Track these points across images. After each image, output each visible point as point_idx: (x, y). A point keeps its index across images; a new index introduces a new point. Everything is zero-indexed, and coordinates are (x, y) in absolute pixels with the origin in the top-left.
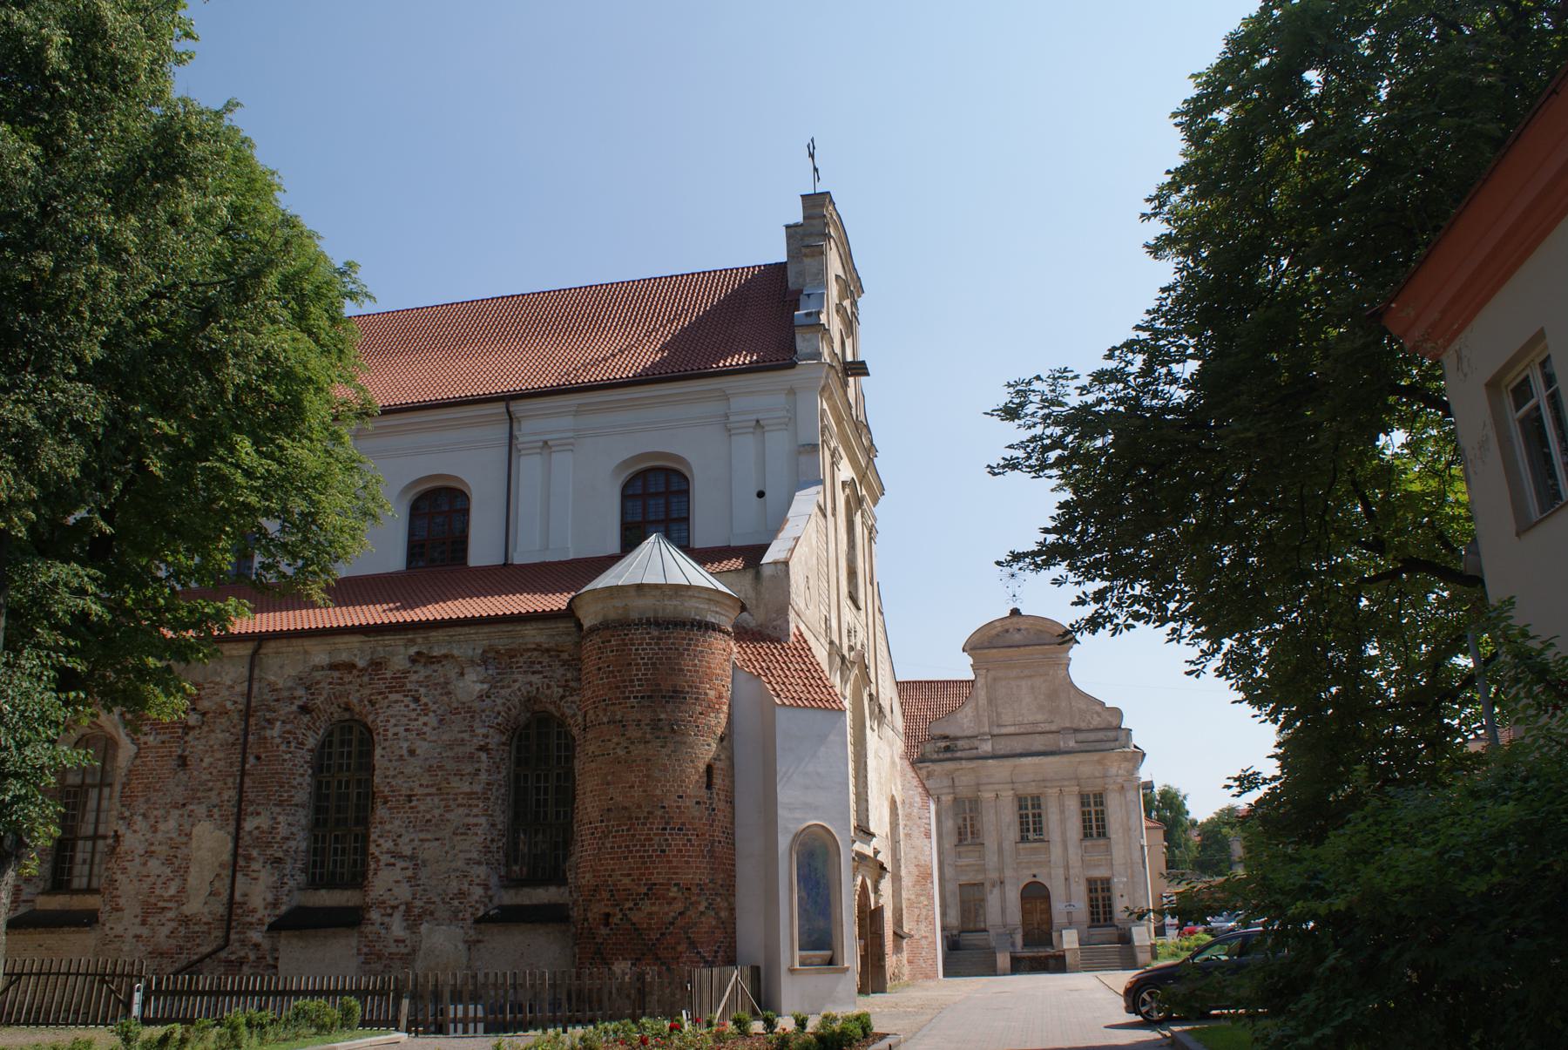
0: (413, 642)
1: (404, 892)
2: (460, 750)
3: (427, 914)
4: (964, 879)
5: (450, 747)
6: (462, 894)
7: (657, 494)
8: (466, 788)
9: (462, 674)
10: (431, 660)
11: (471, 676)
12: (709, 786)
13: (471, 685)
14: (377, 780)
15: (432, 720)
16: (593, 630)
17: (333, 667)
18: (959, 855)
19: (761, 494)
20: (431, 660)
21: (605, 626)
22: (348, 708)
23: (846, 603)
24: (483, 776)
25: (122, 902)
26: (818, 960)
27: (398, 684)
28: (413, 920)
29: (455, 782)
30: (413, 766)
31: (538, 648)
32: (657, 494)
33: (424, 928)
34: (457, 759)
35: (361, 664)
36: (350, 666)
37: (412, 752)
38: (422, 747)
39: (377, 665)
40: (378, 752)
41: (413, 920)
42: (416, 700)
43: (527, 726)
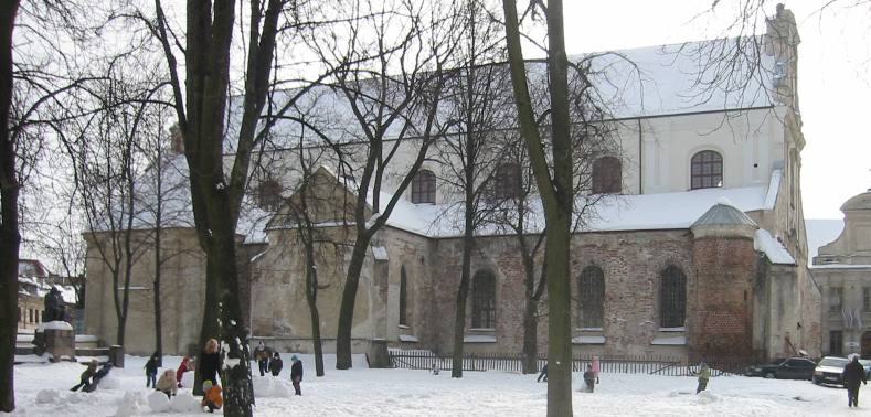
0: (620, 237)
1: (620, 333)
2: (641, 280)
3: (631, 341)
4: (834, 328)
5: (638, 278)
6: (644, 335)
7: (707, 163)
8: (644, 294)
9: (641, 251)
10: (628, 244)
11: (645, 251)
12: (745, 299)
13: (646, 255)
14: (607, 290)
15: (630, 269)
16: (700, 239)
17: (587, 246)
18: (831, 316)
19: (756, 166)
20: (628, 244)
21: (707, 238)
22: (592, 262)
23: (790, 209)
24: (651, 290)
25: (506, 334)
26: (840, 363)
27: (614, 253)
28: (625, 343)
29: (639, 292)
30: (623, 286)
31: (673, 241)
32: (707, 163)
33: (630, 346)
34: (640, 283)
35: (599, 245)
36: (594, 246)
37: (621, 281)
38: (625, 278)
39: (605, 246)
40: (607, 280)
41: (625, 343)
42: (622, 260)
43: (667, 270)
